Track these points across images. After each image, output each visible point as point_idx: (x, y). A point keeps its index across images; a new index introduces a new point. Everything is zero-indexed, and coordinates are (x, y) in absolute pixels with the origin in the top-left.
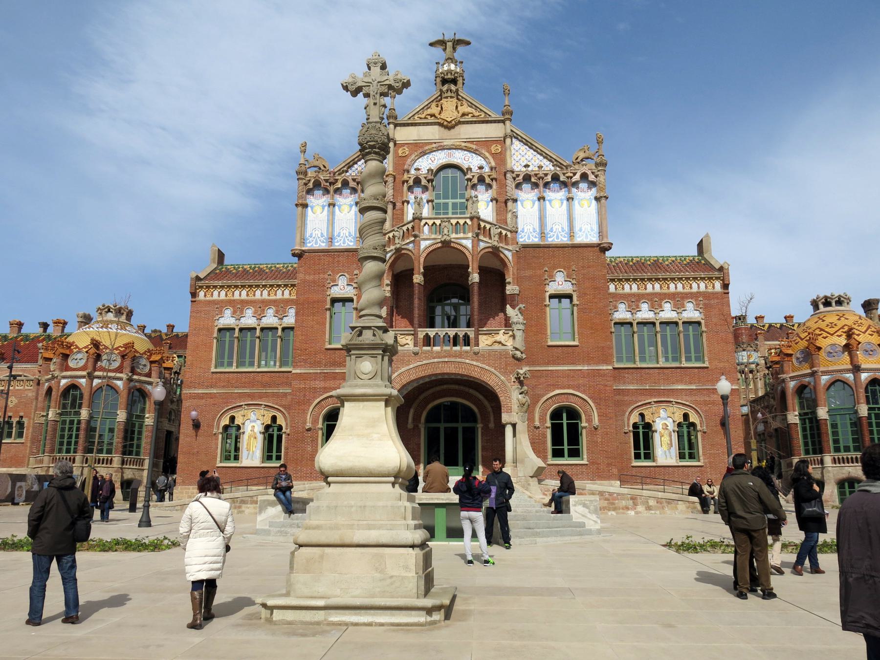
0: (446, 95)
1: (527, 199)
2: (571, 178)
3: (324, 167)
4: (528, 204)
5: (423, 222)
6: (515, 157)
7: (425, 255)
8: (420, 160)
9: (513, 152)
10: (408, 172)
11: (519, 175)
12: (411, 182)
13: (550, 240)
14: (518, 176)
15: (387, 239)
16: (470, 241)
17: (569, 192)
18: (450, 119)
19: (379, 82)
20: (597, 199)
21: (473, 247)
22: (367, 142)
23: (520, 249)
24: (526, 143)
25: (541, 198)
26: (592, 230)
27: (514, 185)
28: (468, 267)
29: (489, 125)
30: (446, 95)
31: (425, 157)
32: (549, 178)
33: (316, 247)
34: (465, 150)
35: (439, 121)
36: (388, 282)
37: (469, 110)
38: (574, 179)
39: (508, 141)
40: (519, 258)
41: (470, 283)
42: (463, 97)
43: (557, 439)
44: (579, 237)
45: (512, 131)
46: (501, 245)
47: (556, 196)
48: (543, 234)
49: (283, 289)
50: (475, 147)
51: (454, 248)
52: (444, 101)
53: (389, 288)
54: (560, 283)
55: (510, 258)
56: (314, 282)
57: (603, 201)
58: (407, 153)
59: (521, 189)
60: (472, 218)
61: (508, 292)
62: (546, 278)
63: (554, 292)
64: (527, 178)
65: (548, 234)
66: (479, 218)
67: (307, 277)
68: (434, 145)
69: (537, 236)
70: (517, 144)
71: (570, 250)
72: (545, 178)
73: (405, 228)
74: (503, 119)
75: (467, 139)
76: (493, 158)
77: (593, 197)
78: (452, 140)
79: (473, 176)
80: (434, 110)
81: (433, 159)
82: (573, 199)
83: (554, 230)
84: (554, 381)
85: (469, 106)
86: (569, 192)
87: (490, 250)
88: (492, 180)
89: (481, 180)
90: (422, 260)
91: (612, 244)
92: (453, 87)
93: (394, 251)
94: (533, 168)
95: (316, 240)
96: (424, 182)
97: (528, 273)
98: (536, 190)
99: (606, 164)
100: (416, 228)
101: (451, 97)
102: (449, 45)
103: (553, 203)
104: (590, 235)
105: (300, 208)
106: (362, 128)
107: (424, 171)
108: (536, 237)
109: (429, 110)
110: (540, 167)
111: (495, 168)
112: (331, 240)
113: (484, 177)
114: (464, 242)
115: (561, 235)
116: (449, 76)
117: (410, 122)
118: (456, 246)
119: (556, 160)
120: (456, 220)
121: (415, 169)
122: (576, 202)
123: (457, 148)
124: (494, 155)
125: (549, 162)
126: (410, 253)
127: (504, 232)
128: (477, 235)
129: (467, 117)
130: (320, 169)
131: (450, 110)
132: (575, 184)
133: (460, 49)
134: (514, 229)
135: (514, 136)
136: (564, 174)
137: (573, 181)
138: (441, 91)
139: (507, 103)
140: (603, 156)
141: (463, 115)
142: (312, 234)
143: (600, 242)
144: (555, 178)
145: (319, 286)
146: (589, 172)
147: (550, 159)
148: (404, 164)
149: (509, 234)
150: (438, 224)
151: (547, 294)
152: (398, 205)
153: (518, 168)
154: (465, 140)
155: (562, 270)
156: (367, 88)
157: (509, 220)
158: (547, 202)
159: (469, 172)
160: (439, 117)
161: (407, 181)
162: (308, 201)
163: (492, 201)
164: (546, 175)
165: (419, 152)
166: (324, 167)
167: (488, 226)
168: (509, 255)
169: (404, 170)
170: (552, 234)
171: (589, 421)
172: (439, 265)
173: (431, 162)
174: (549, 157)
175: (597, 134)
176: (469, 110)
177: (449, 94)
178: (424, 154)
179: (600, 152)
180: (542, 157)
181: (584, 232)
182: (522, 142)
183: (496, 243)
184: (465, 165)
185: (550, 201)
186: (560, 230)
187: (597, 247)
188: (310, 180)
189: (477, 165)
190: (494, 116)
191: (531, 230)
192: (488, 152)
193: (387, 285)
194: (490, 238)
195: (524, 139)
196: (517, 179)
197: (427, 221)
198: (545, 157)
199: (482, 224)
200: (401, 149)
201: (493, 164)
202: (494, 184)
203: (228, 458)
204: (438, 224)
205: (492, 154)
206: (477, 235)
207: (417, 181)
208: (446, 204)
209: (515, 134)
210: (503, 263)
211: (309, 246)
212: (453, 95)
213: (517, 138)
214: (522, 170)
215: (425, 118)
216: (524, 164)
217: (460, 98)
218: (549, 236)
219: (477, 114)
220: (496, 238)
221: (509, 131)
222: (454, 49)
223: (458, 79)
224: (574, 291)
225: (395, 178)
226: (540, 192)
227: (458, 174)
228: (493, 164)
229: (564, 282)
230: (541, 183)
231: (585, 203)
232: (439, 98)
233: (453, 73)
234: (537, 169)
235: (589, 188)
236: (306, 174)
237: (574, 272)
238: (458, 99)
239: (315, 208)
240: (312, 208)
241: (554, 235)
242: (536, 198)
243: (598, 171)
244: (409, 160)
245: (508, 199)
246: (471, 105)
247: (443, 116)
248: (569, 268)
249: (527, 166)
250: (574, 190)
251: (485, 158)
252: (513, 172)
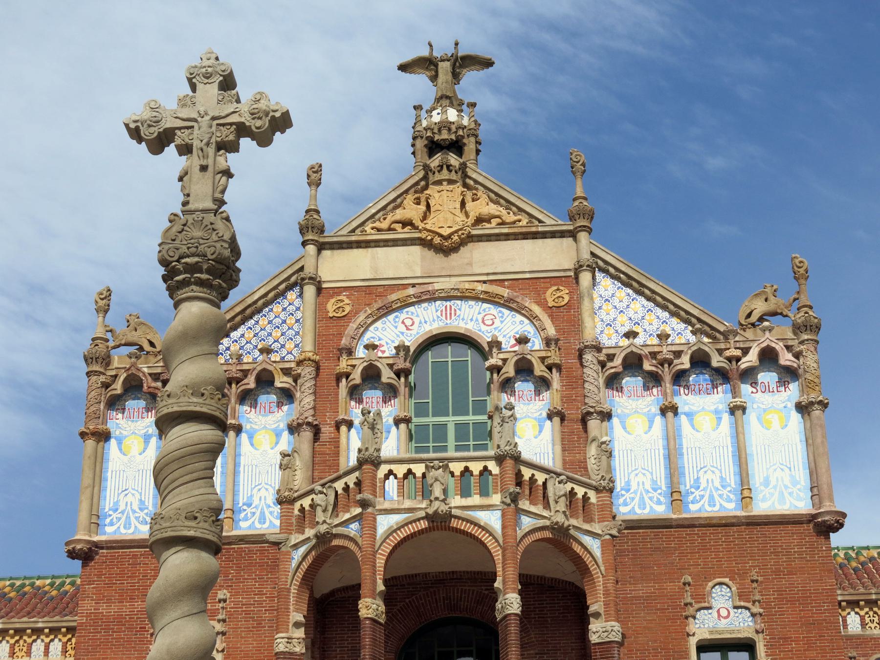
0: (438, 177)
2: (738, 359)
3: (152, 344)
4: (637, 423)
5: (383, 469)
6: (603, 314)
7: (387, 549)
8: (378, 324)
9: (598, 302)
10: (350, 352)
11: (614, 355)
12: (356, 377)
13: (693, 507)
14: (611, 358)
15: (296, 512)
16: (498, 514)
17: (735, 393)
18: (449, 231)
19: (214, 118)
20: (802, 408)
21: (504, 527)
22: (181, 257)
23: (619, 531)
24: (627, 282)
25: (669, 410)
26: (795, 483)
27: (601, 381)
28: (493, 577)
29: (540, 242)
30: (438, 177)
31: (391, 317)
32: (685, 362)
33: (127, 534)
34: (484, 301)
35: (423, 235)
36: (300, 618)
37: (493, 209)
38: (744, 364)
39: (585, 278)
40: (620, 554)
41: (499, 617)
42: (476, 182)
44: (764, 500)
45: (593, 254)
46: (573, 522)
48: (675, 496)
49: (47, 640)
51: (457, 530)
52: (432, 190)
53: (300, 633)
54: (724, 613)
55: (597, 553)
56: (119, 620)
57: (817, 413)
58: (348, 309)
59: (620, 389)
60: (500, 459)
61: (594, 639)
62: (689, 600)
63: (708, 636)
64: (633, 363)
65: (688, 493)
66: (517, 459)
67: (103, 608)
68: (411, 291)
69: (662, 499)
70: (606, 284)
71: (745, 532)
72: (676, 362)
73: (339, 486)
74: (571, 228)
75: (488, 274)
76: (551, 316)
77: (791, 405)
78: (454, 280)
79: (505, 361)
80: (411, 210)
81: (408, 322)
82: (744, 409)
83: (703, 485)
85: (492, 201)
86: (735, 393)
87: (548, 534)
88: (550, 368)
89: (524, 368)
90: (380, 562)
91: (844, 515)
92: (454, 160)
93: (314, 541)
94: (646, 340)
95: (128, 517)
96: (387, 376)
97: (642, 589)
98: (655, 390)
99: (818, 328)
100: (366, 484)
101: (451, 182)
102: (445, 67)
103: (697, 419)
104: (791, 494)
105: (90, 443)
106: (169, 224)
107: (389, 351)
108: (659, 503)
109: (398, 211)
110: (663, 337)
111: (557, 341)
113: (530, 362)
114: (483, 517)
115: (721, 496)
116: (445, 135)
117: (353, 238)
118: (463, 526)
119: (699, 320)
120: (463, 464)
121: (367, 347)
122: (751, 417)
123: (465, 296)
124: (553, 312)
125: (683, 325)
126: (352, 546)
127: (580, 491)
128: (515, 498)
129: (488, 225)
130: (141, 349)
132: (748, 375)
133: (470, 77)
134: (604, 483)
135: (598, 266)
136: (720, 352)
137: (743, 366)
138: (426, 168)
139: (579, 192)
140: (811, 307)
141: (479, 220)
142: (117, 503)
143: (814, 512)
144: (700, 361)
145: (130, 629)
146: (779, 347)
147: (687, 318)
148: (340, 335)
149: (592, 494)
150: (419, 474)
151: (693, 642)
152: (327, 431)
153: (610, 339)
154: (485, 278)
155: (726, 580)
156: (187, 132)
157: (591, 463)
158: (683, 418)
159: (495, 350)
160: (421, 226)
161: (347, 375)
162: (111, 425)
163: (550, 417)
164: (678, 354)
165: (376, 306)
166: (152, 344)
167: (540, 478)
168: (594, 546)
169: (340, 350)
170: (697, 493)
172: (426, 575)
173: (402, 328)
174: (682, 313)
175: (793, 259)
176: (493, 209)
177: (445, 174)
178: (387, 310)
179: (804, 300)
180: (667, 314)
181: (775, 487)
182: (618, 279)
183: (560, 518)
184: (484, 336)
185: (689, 415)
186: (717, 484)
187: (809, 522)
188: (116, 376)
189: (512, 334)
190: (550, 222)
191: (648, 486)
192: (538, 303)
193: (297, 625)
194: (547, 506)
195: (624, 273)
196: (609, 365)
197: (393, 467)
198: (673, 314)
199: (527, 473)
200: (333, 301)
201: (551, 331)
202: (555, 378)
204: (419, 474)
205: (549, 310)
206: (515, 498)
207: (371, 375)
208: (441, 429)
209: (600, 263)
210: (581, 566)
211: (110, 532)
212: (453, 176)
213: (606, 272)
214: (621, 344)
215: (390, 229)
216: (626, 329)
217: (471, 183)
218: (691, 498)
220: (562, 506)
221: (586, 255)
222: (456, 76)
223: (465, 141)
224: (757, 632)
225: (318, 369)
226: (665, 394)
227: (470, 355)
228: (551, 331)
229: (732, 611)
230: (667, 374)
231: (775, 419)
232: (423, 183)
233: (453, 128)
234: (655, 341)
235: (783, 383)
236: (106, 361)
237: (755, 585)
238: (465, 185)
239: (126, 442)
240: (120, 442)
241: (702, 497)
242: (655, 410)
243: (802, 343)
244: (353, 326)
245: (589, 414)
246: (497, 198)
247: (430, 224)
248: (743, 574)
249: (631, 335)
250: (746, 388)
251: (532, 318)
252: (598, 349)
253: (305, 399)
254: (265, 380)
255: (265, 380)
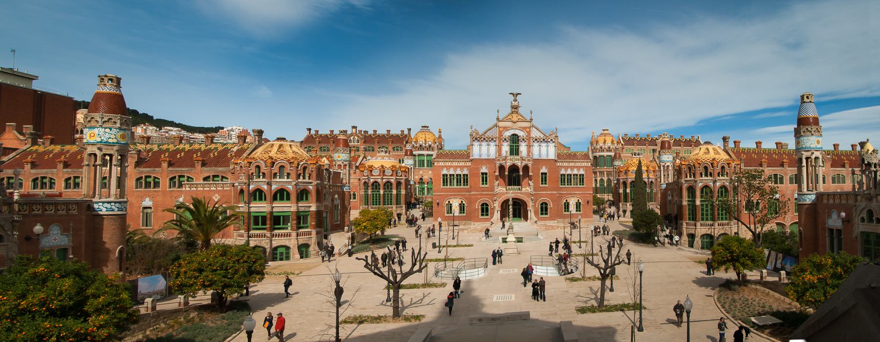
1: (536, 145)
4: (536, 147)
32: (542, 140)
37: (521, 117)
43: (542, 210)
47: (544, 145)
50: (522, 129)
64: (536, 140)
80: (510, 117)
84: (541, 196)
102: (515, 95)
112: (480, 155)
131: (515, 118)
152: (500, 146)
171: (550, 206)
184: (519, 135)
203: (448, 213)
208: (513, 146)
219: (523, 119)
222: (517, 96)
253: (497, 142)
254: (492, 139)
255: (492, 139)
